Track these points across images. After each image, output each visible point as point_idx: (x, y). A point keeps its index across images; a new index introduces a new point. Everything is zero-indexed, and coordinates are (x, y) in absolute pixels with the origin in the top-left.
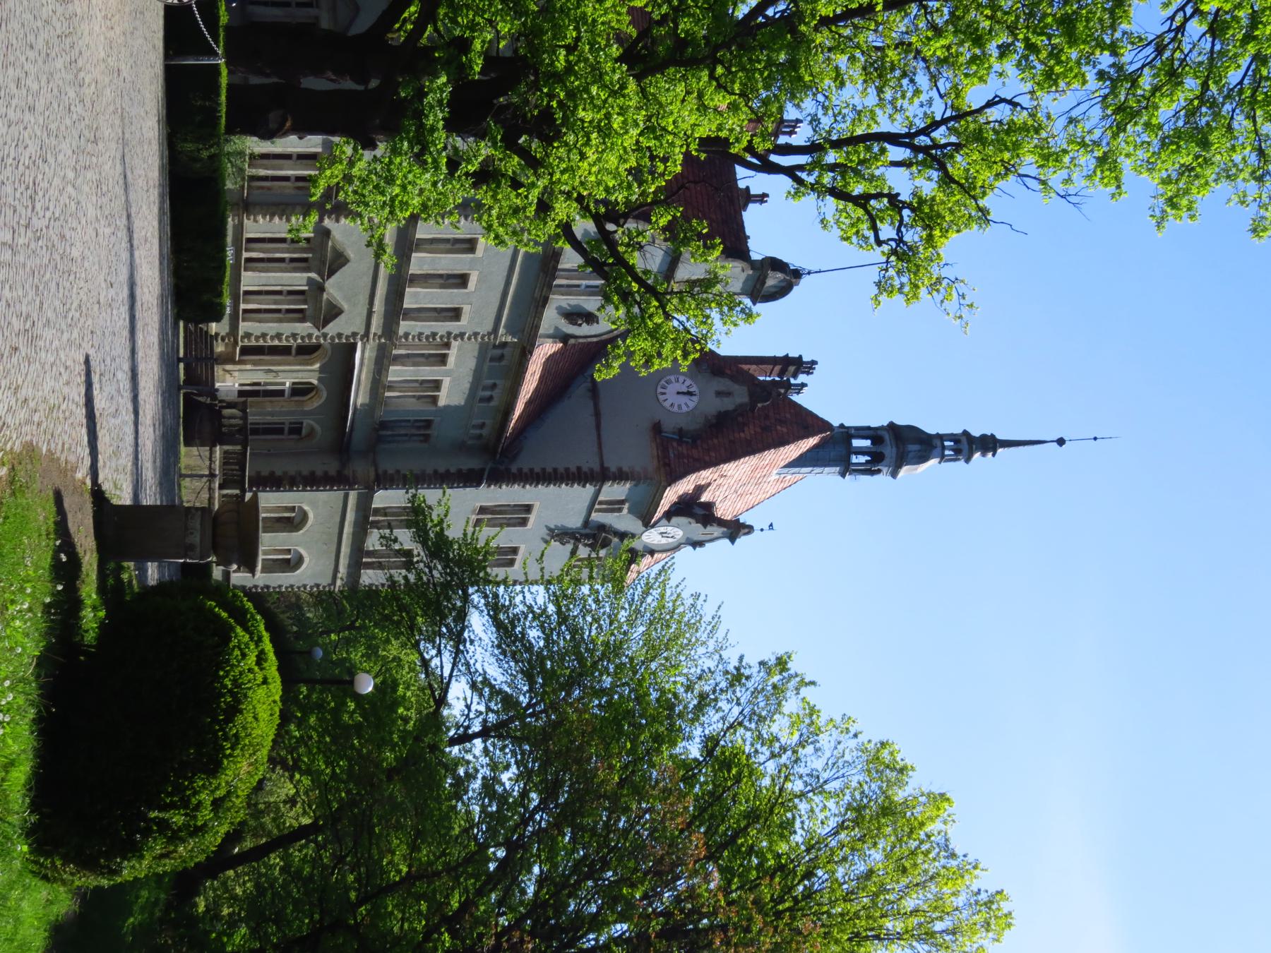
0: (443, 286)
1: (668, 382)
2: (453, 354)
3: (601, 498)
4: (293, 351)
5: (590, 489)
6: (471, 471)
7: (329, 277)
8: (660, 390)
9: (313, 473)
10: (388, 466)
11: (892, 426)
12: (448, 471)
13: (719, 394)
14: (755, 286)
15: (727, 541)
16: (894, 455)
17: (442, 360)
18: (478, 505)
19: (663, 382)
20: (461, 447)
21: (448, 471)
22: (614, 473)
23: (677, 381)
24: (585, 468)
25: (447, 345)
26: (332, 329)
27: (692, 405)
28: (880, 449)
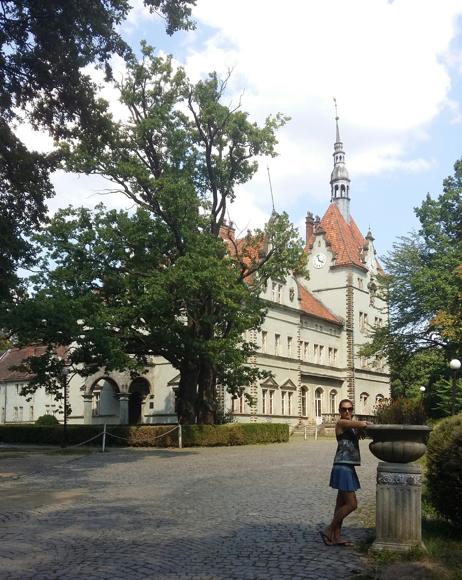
2: (304, 340)
5: (355, 291)
8: (318, 267)
11: (331, 183)
13: (319, 246)
17: (306, 344)
23: (315, 261)
24: (347, 293)
27: (323, 255)
28: (340, 186)
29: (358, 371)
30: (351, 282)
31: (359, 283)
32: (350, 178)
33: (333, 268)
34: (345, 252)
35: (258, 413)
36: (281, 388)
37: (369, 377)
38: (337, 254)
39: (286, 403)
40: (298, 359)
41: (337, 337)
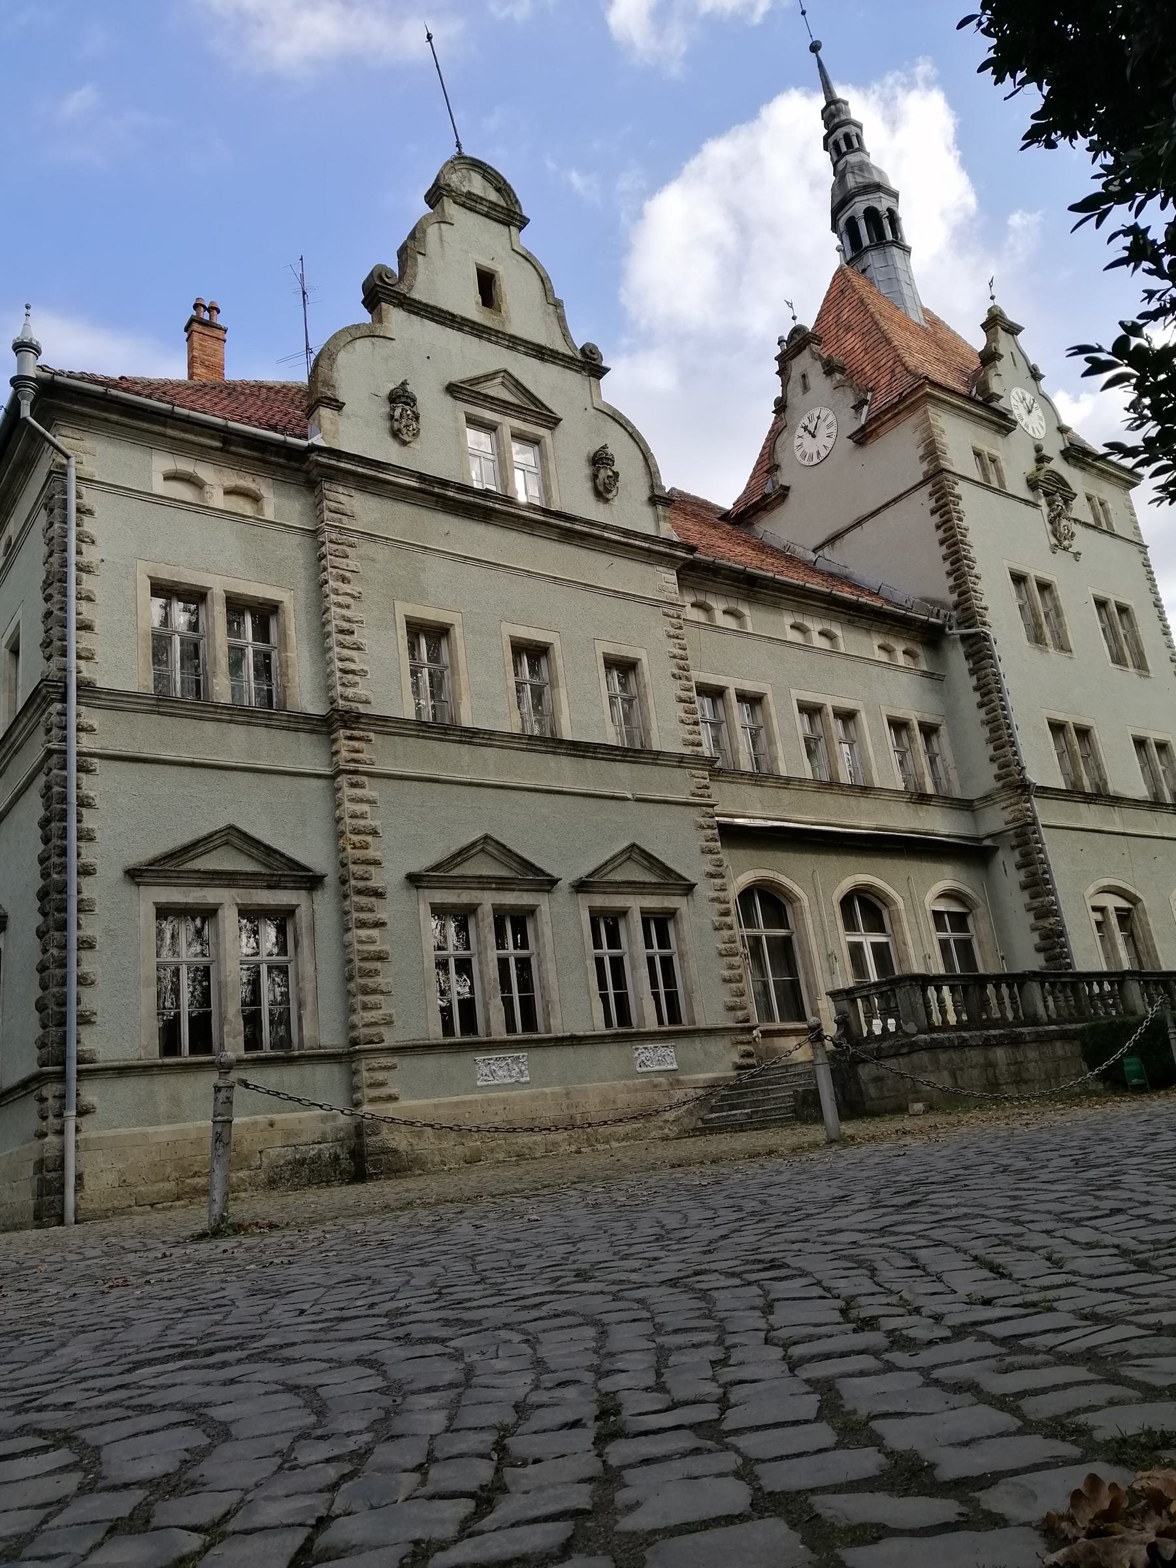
0: (553, 683)
1: (804, 456)
3: (978, 477)
4: (781, 932)
5: (961, 488)
6: (967, 658)
7: (539, 871)
8: (816, 461)
9: (1024, 887)
10: (985, 779)
12: (976, 689)
14: (486, 215)
15: (1019, 337)
16: (865, 197)
18: (1027, 644)
19: (806, 462)
20: (935, 677)
21: (976, 689)
22: (930, 463)
24: (932, 504)
25: (715, 693)
26: (692, 867)
29: (1045, 792)
30: (937, 458)
31: (984, 470)
32: (894, 185)
33: (862, 438)
34: (897, 371)
35: (391, 1038)
36: (582, 887)
37: (1116, 819)
38: (872, 390)
39: (634, 968)
40: (688, 750)
41: (925, 674)
